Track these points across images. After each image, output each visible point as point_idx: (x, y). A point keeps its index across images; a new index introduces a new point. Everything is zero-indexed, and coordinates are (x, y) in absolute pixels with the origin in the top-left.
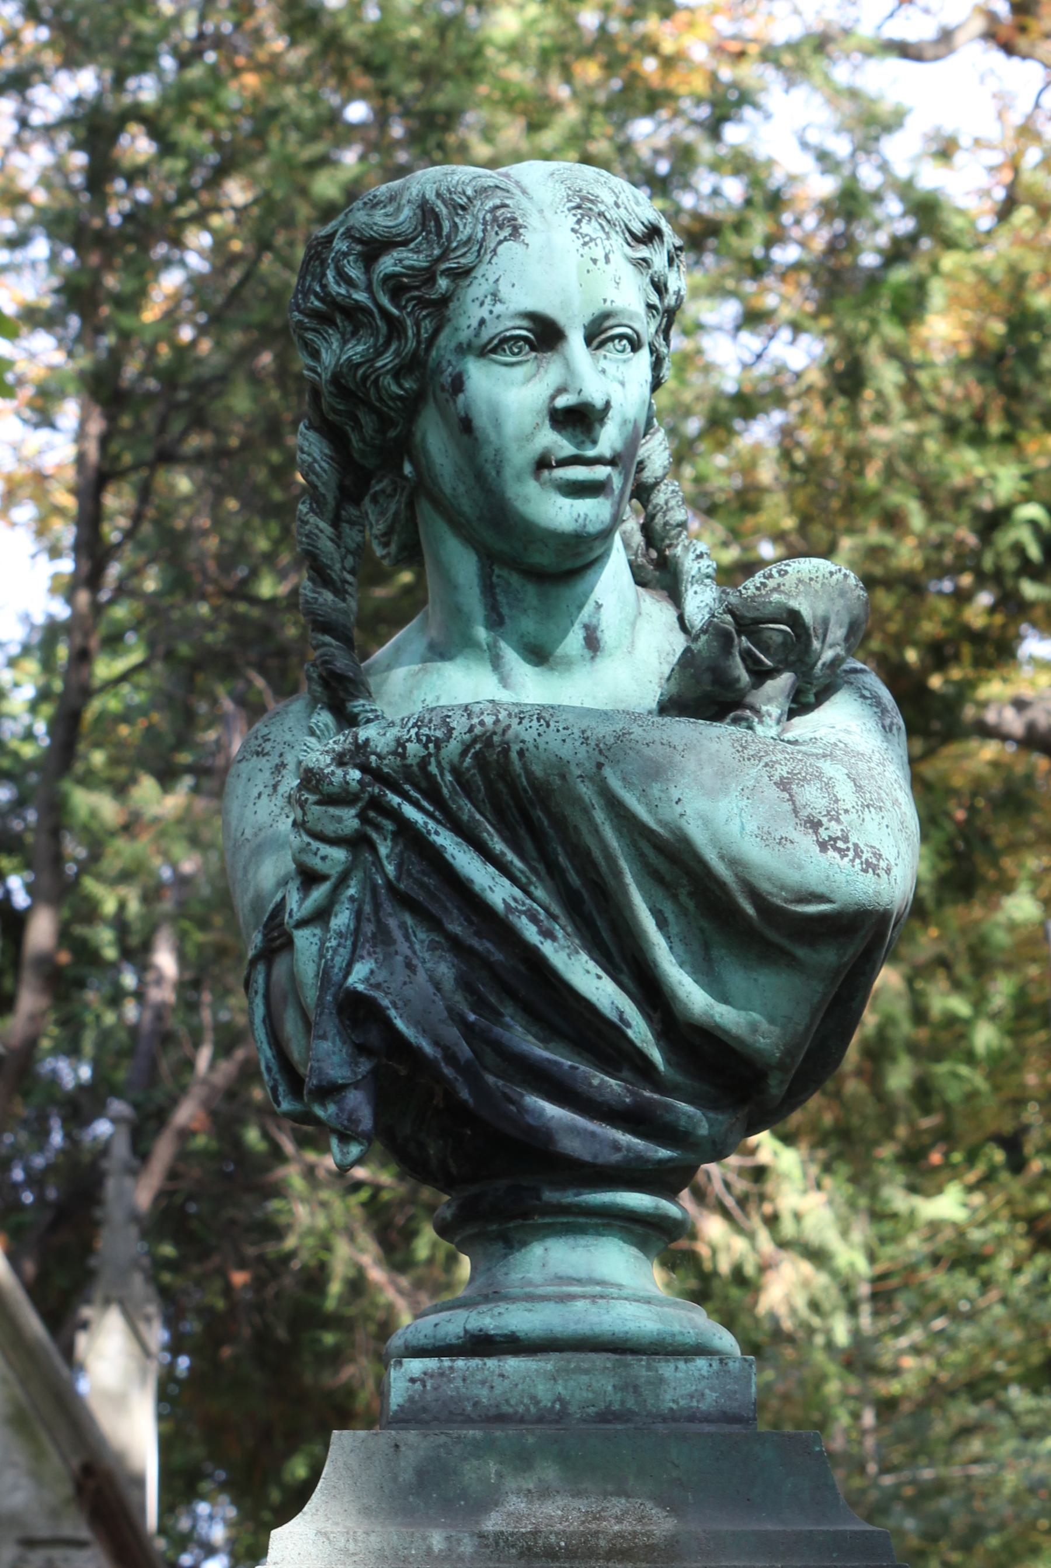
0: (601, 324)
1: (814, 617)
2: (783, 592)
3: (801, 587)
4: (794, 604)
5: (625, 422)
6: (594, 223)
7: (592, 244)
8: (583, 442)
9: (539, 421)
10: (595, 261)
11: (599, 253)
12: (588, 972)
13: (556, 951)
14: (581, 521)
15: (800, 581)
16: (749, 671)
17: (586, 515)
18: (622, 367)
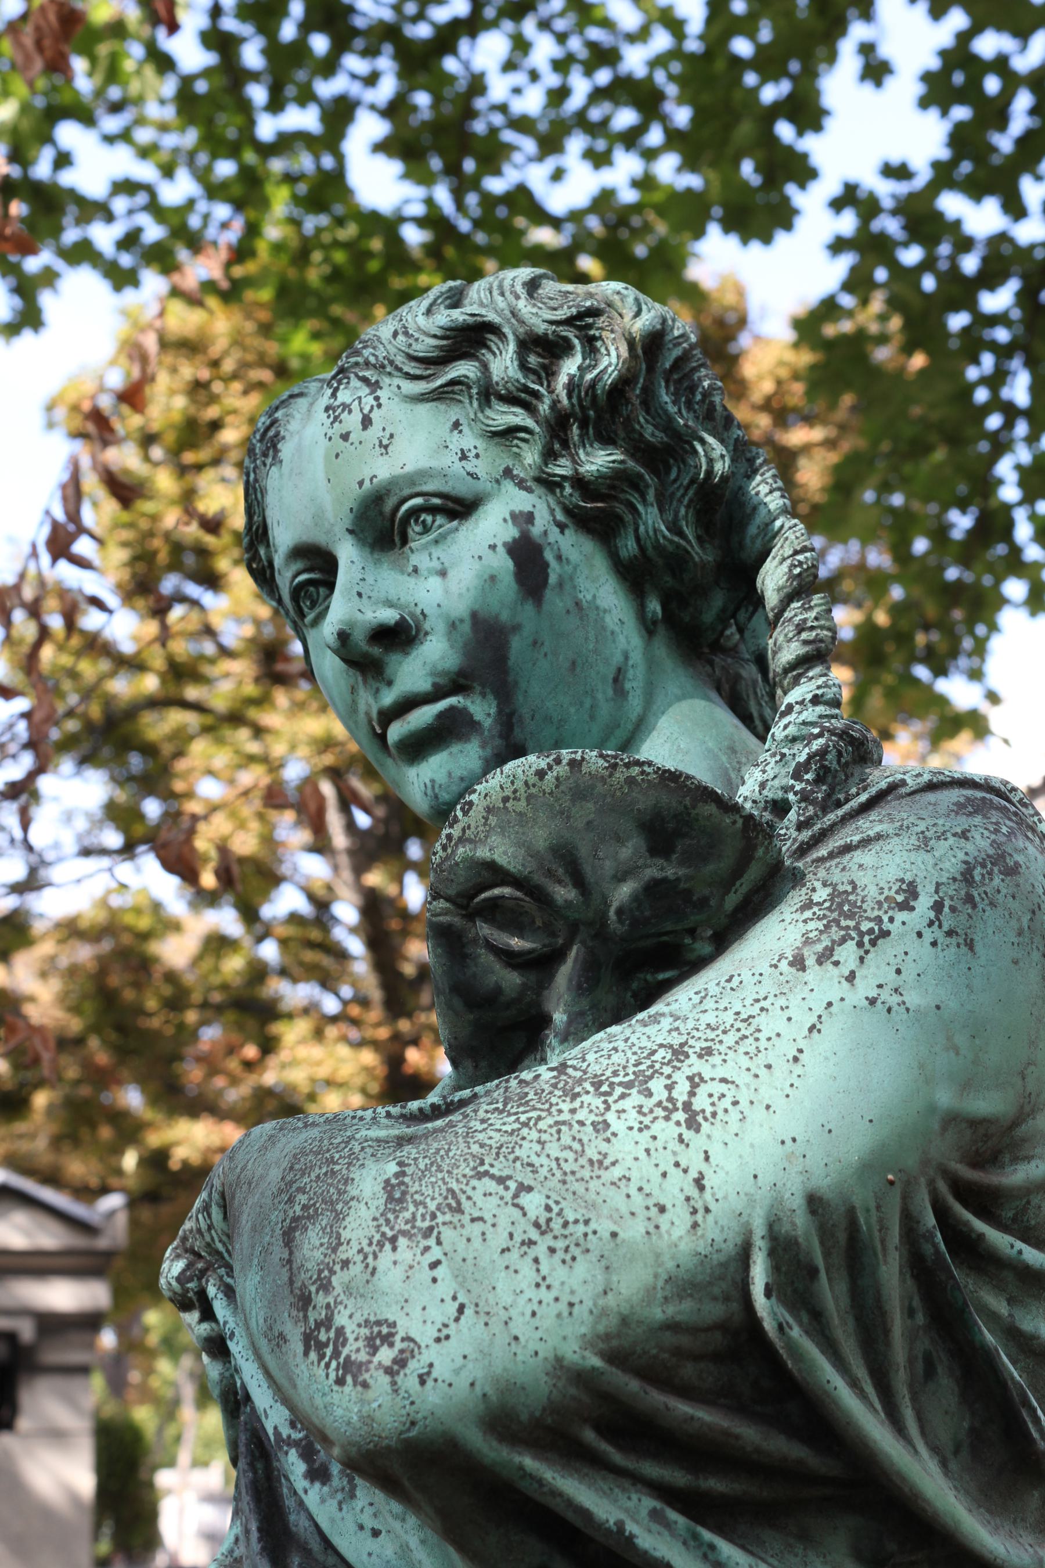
0: (381, 513)
2: (470, 841)
3: (493, 820)
4: (483, 853)
5: (453, 626)
6: (355, 382)
7: (345, 416)
8: (377, 691)
9: (352, 681)
10: (345, 437)
11: (352, 421)
12: (361, 1527)
13: (323, 1501)
14: (429, 792)
15: (489, 810)
17: (433, 781)
18: (436, 552)
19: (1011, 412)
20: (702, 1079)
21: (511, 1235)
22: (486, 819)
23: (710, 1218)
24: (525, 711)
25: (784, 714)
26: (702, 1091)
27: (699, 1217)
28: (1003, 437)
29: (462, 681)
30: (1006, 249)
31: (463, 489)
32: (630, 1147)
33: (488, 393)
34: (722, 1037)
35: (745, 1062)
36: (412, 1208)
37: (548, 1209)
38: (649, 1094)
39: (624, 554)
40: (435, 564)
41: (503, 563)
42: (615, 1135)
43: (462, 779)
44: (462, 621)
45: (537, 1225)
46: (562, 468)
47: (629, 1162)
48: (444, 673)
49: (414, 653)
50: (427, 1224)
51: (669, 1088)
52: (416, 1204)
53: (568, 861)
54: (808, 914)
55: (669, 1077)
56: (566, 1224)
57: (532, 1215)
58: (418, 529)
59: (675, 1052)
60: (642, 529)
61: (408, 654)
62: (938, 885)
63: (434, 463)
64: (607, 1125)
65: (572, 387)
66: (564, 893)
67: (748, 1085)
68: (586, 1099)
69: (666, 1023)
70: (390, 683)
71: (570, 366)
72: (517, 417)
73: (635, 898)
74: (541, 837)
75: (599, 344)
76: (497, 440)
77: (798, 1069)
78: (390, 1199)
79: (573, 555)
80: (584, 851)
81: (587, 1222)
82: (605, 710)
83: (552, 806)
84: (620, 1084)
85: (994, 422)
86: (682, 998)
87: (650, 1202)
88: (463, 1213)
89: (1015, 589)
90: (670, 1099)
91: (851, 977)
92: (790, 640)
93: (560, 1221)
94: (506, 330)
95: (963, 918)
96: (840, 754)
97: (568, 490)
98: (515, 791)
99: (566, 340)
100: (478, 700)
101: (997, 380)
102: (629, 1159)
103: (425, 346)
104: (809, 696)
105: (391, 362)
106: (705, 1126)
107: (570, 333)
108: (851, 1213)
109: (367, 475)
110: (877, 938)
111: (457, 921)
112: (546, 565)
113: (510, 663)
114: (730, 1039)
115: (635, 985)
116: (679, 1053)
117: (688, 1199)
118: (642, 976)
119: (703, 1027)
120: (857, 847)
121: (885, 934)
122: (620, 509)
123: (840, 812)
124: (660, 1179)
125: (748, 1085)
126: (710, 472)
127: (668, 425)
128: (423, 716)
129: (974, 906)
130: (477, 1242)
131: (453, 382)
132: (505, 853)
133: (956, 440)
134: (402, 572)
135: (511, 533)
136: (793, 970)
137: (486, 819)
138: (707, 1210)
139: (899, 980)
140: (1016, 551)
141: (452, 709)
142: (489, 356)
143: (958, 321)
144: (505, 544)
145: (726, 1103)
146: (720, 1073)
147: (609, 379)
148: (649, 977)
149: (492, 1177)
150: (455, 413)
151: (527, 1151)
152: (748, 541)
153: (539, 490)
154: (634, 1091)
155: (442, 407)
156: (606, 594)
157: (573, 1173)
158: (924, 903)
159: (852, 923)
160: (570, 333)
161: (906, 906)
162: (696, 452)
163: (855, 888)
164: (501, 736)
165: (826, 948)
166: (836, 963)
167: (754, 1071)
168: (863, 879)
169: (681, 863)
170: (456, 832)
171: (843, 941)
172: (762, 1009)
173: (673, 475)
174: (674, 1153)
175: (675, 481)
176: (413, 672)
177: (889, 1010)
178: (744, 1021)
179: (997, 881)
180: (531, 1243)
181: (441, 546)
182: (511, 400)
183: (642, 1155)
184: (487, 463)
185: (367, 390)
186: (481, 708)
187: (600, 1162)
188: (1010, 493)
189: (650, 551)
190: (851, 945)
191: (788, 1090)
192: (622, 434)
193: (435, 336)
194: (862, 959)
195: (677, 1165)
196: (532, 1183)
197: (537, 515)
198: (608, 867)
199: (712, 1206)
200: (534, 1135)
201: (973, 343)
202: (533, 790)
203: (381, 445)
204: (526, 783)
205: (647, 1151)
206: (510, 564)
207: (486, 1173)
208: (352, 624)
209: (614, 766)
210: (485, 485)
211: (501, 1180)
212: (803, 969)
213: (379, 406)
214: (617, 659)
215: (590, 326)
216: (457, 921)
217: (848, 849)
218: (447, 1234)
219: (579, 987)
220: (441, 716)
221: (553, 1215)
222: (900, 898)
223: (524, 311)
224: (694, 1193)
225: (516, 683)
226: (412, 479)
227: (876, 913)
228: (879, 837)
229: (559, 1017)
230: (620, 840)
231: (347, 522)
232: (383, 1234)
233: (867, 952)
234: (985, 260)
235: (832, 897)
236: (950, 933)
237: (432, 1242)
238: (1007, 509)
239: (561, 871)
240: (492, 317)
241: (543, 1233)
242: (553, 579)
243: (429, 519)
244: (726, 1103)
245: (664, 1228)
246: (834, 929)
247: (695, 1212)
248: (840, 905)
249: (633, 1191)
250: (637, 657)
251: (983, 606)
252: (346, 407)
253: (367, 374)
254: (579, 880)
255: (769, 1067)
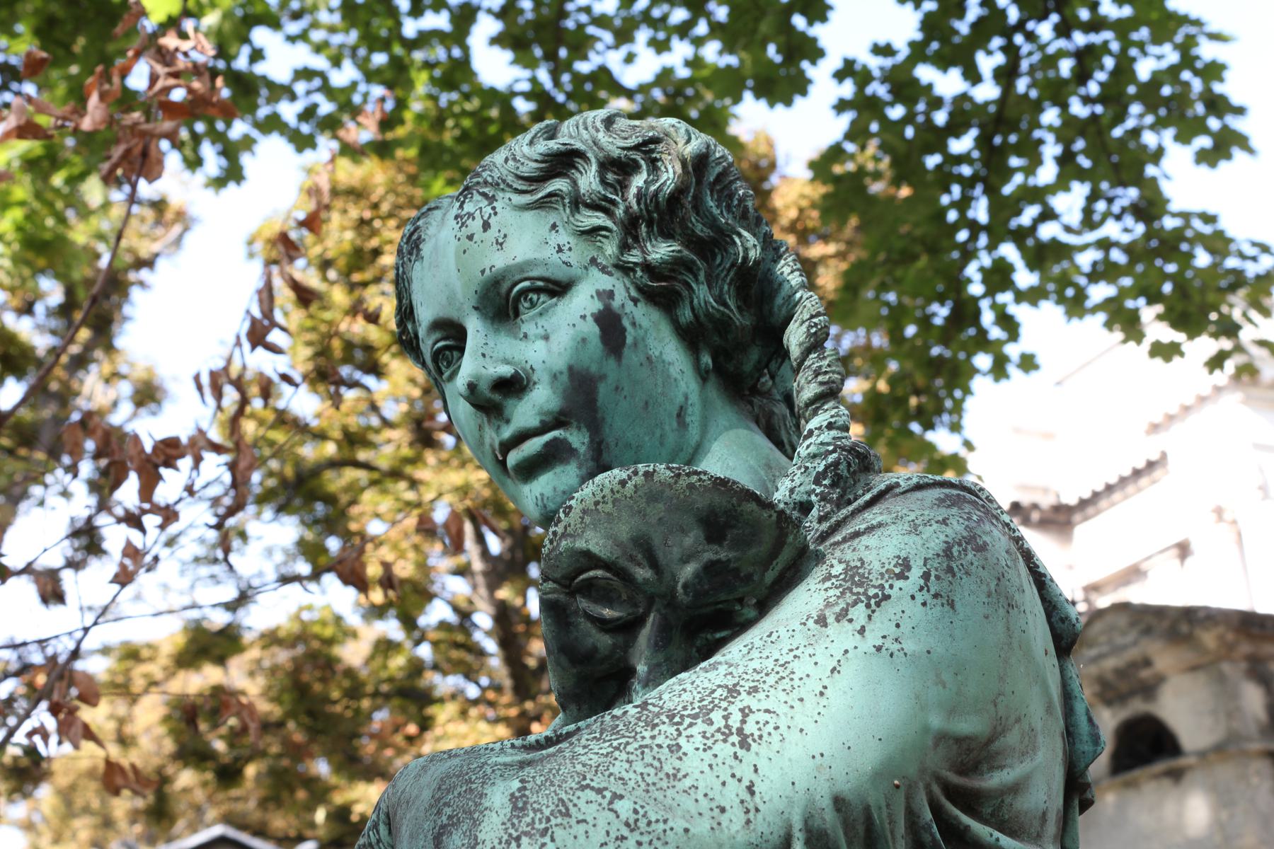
0: (499, 294)
1: (619, 544)
2: (571, 535)
3: (587, 519)
4: (580, 544)
5: (554, 377)
6: (477, 197)
7: (470, 222)
8: (499, 427)
9: (479, 421)
10: (470, 238)
11: (475, 225)
14: (540, 503)
15: (584, 512)
16: (607, 631)
17: (542, 495)
18: (541, 322)
19: (975, 228)
20: (751, 711)
21: (608, 833)
22: (582, 518)
23: (760, 816)
24: (611, 440)
25: (806, 437)
26: (751, 719)
27: (751, 815)
28: (970, 247)
29: (563, 418)
30: (967, 106)
31: (560, 274)
32: (697, 763)
33: (577, 202)
34: (765, 678)
35: (783, 697)
36: (531, 814)
37: (636, 811)
38: (712, 723)
39: (682, 320)
40: (540, 331)
41: (592, 329)
42: (685, 754)
43: (564, 492)
44: (561, 373)
45: (627, 824)
46: (634, 257)
47: (697, 774)
48: (549, 413)
49: (526, 398)
50: (543, 826)
51: (726, 718)
52: (535, 811)
53: (645, 549)
54: (828, 584)
55: (726, 709)
56: (649, 823)
57: (623, 817)
58: (527, 305)
59: (730, 691)
60: (696, 301)
61: (521, 399)
62: (926, 560)
63: (537, 255)
64: (679, 747)
65: (640, 196)
66: (642, 573)
67: (786, 714)
68: (662, 727)
69: (722, 669)
70: (508, 421)
71: (638, 181)
72: (599, 219)
73: (697, 575)
74: (624, 530)
75: (659, 164)
76: (584, 237)
77: (823, 701)
78: (515, 808)
79: (645, 322)
80: (657, 541)
81: (665, 821)
82: (671, 438)
83: (631, 507)
84: (689, 716)
85: (962, 236)
86: (734, 651)
87: (714, 805)
88: (571, 817)
89: (983, 361)
90: (727, 726)
91: (862, 631)
92: (809, 382)
93: (645, 821)
94: (590, 155)
95: (945, 584)
96: (849, 465)
97: (639, 273)
98: (604, 497)
99: (635, 161)
100: (575, 432)
101: (963, 204)
102: (697, 772)
103: (529, 168)
104: (825, 424)
105: (504, 181)
106: (754, 746)
107: (637, 156)
108: (867, 810)
109: (487, 265)
110: (881, 601)
111: (562, 597)
112: (624, 330)
113: (599, 404)
114: (771, 680)
115: (698, 643)
116: (733, 691)
117: (742, 802)
118: (703, 635)
119: (750, 671)
120: (864, 533)
121: (887, 597)
122: (678, 286)
123: (851, 508)
124: (720, 787)
125: (786, 714)
126: (746, 258)
127: (713, 223)
128: (534, 445)
129: (954, 575)
130: (582, 838)
131: (550, 195)
132: (597, 544)
133: (934, 249)
134: (516, 338)
135: (597, 306)
136: (818, 626)
137: (582, 518)
138: (757, 810)
139: (897, 632)
140: (983, 333)
141: (555, 439)
142: (577, 175)
143: (932, 161)
144: (592, 315)
145: (770, 728)
146: (764, 705)
147: (668, 190)
148: (709, 636)
149: (593, 788)
150: (552, 217)
151: (619, 768)
152: (776, 309)
153: (618, 274)
154: (699, 721)
155: (543, 213)
156: (669, 351)
157: (654, 784)
158: (916, 573)
159: (861, 590)
160: (637, 156)
161: (902, 576)
162: (735, 243)
163: (863, 563)
164: (593, 459)
165: (842, 609)
166: (851, 621)
167: (790, 703)
168: (869, 557)
169: (731, 548)
170: (560, 529)
171: (855, 603)
172: (795, 657)
173: (718, 261)
174: (731, 767)
175: (720, 265)
176: (525, 412)
177: (891, 655)
178: (782, 666)
179: (970, 556)
180: (623, 838)
181: (544, 317)
182: (594, 207)
183: (707, 769)
184: (578, 254)
185: (486, 202)
186: (577, 438)
187: (675, 776)
188: (976, 289)
189: (702, 318)
190: (861, 606)
191: (817, 717)
192: (678, 231)
193: (536, 161)
194: (870, 617)
195: (733, 776)
196: (623, 793)
197: (616, 293)
198: (676, 552)
199: (761, 807)
200: (624, 756)
201: (944, 178)
202: (618, 496)
203: (497, 243)
204: (612, 490)
205: (711, 766)
206: (596, 329)
207: (588, 786)
208: (478, 377)
209: (679, 475)
210: (576, 271)
211: (599, 791)
212: (826, 625)
213: (496, 214)
214: (680, 399)
215: (652, 151)
216: (562, 597)
217: (857, 534)
218: (559, 833)
219: (656, 644)
220: (547, 445)
221: (639, 816)
222: (897, 570)
223: (603, 140)
224: (747, 797)
225: (604, 419)
226: (521, 267)
227: (880, 582)
228: (880, 525)
229: (642, 668)
230: (683, 531)
231: (473, 302)
232: (510, 835)
233: (873, 612)
234: (951, 114)
235: (846, 571)
236: (936, 596)
237: (547, 839)
238: (975, 300)
239: (640, 556)
240: (579, 145)
241: (632, 831)
242: (629, 340)
243: (535, 297)
244: (770, 728)
245: (724, 824)
246: (848, 594)
247: (747, 811)
248: (852, 577)
249: (700, 797)
250: (694, 398)
251: (959, 375)
252: (471, 215)
253: (486, 190)
254: (654, 564)
255: (801, 700)
